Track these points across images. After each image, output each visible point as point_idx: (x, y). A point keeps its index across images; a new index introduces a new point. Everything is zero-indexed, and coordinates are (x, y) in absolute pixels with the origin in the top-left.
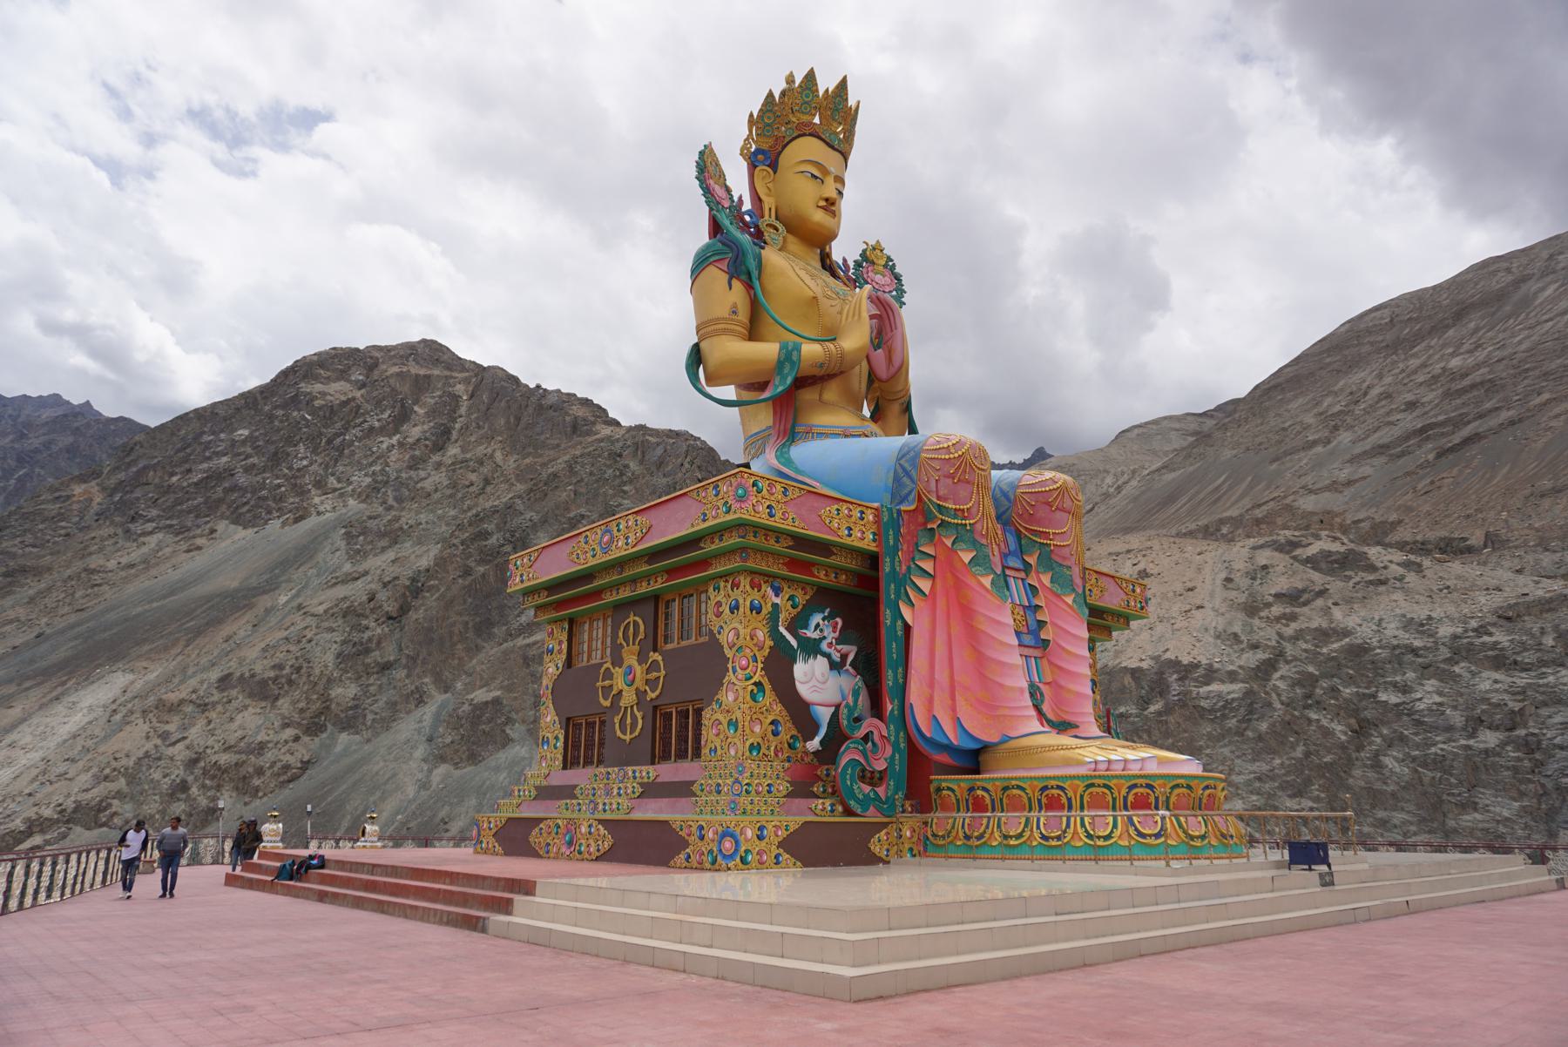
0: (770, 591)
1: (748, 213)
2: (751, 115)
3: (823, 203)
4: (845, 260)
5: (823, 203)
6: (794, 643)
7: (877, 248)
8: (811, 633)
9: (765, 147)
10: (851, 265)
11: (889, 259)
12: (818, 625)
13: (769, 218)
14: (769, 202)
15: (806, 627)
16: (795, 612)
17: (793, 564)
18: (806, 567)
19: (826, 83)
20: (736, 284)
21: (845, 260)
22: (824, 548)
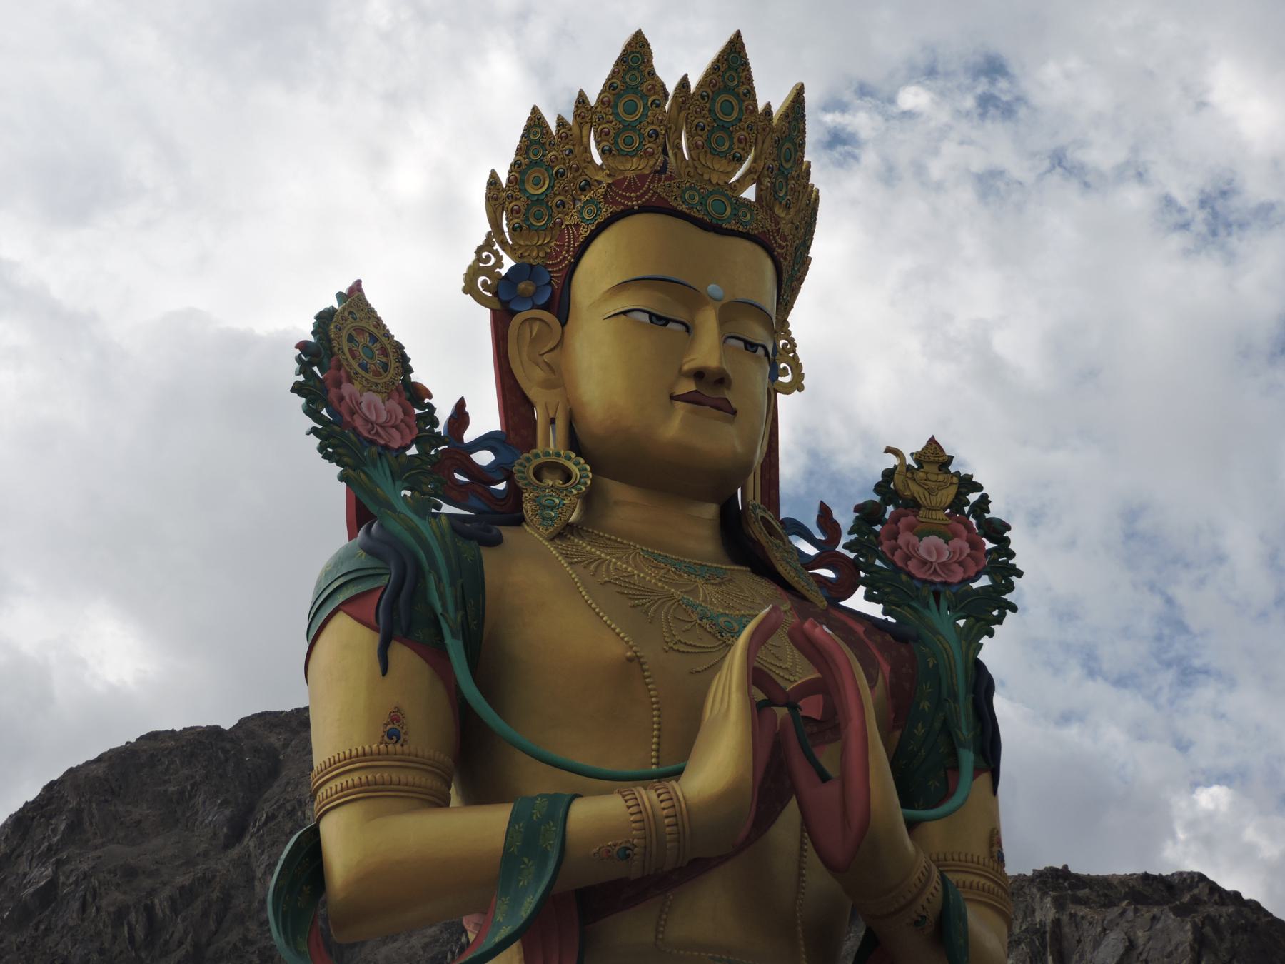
1: (485, 442)
2: (493, 181)
3: (688, 386)
4: (825, 515)
5: (688, 386)
7: (934, 457)
9: (534, 257)
10: (845, 519)
11: (968, 484)
13: (551, 442)
19: (681, 62)
20: (401, 654)
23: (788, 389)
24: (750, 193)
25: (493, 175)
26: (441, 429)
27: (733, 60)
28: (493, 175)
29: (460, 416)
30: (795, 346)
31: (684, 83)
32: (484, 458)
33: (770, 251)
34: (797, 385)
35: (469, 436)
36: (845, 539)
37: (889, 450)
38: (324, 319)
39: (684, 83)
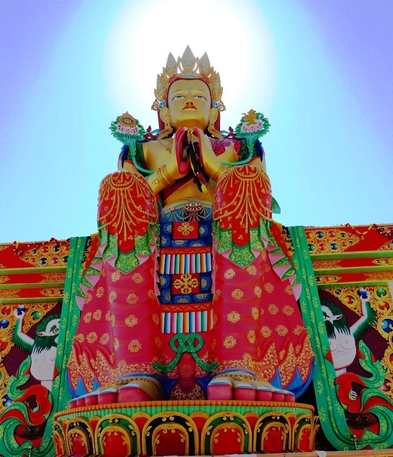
0: (15, 312)
4: (230, 129)
6: (30, 341)
7: (252, 112)
8: (47, 333)
10: (234, 128)
11: (259, 114)
12: (55, 327)
14: (166, 120)
15: (44, 330)
16: (35, 322)
17: (23, 293)
18: (35, 292)
21: (230, 129)
22: (37, 277)
23: (222, 110)
24: (198, 72)
25: (155, 89)
26: (146, 131)
27: (188, 51)
28: (155, 89)
29: (150, 128)
30: (223, 103)
31: (179, 57)
32: (154, 134)
33: (203, 81)
34: (224, 109)
35: (152, 130)
36: (234, 130)
37: (243, 114)
38: (118, 118)
39: (179, 57)
